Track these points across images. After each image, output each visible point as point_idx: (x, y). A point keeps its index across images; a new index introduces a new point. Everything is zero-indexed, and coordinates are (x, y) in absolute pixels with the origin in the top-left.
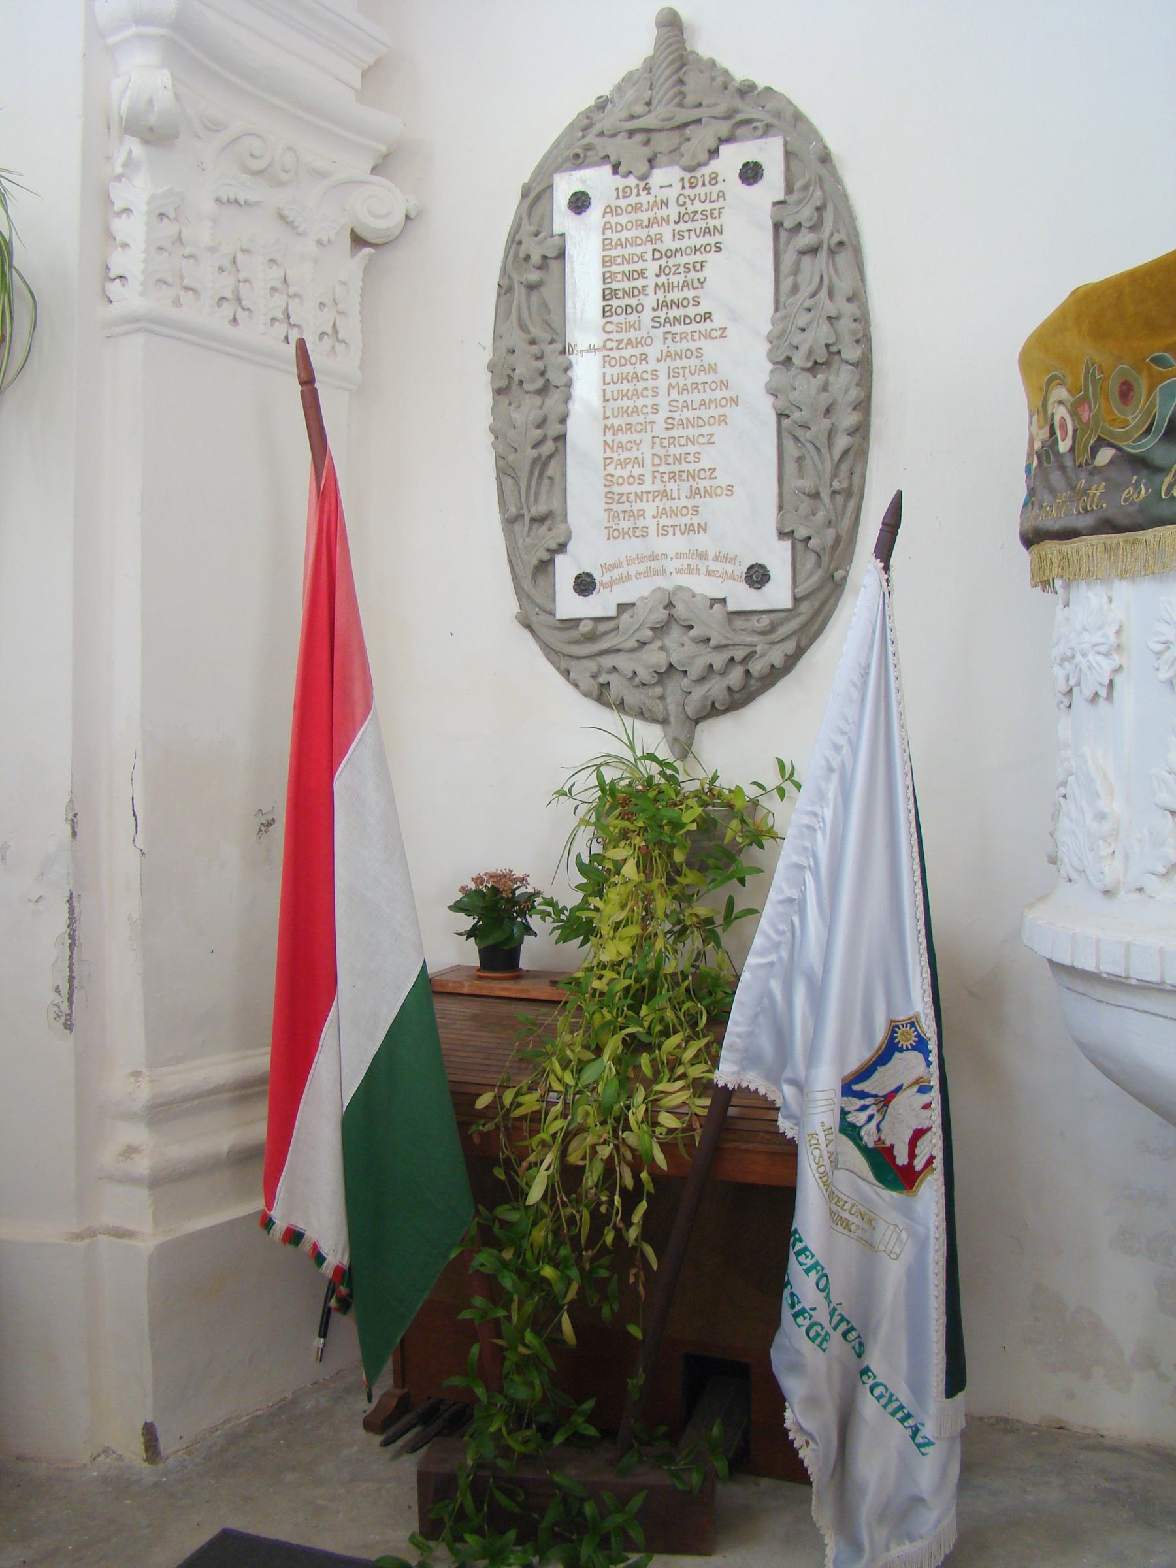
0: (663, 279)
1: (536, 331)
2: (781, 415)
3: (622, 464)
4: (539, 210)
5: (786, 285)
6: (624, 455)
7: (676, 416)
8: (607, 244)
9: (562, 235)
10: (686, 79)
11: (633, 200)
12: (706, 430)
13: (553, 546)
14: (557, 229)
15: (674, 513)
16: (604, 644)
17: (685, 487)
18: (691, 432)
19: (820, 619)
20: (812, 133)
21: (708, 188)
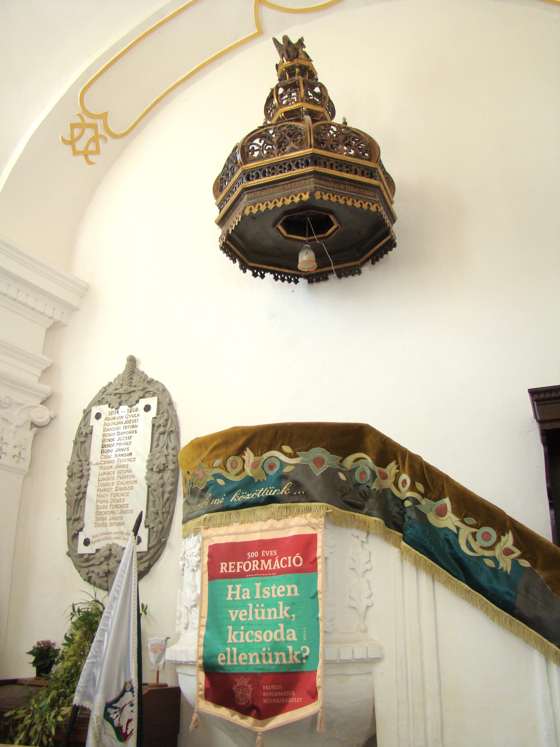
0: (119, 442)
1: (82, 458)
2: (149, 487)
3: (101, 502)
4: (87, 418)
5: (155, 444)
6: (103, 499)
7: (119, 486)
8: (105, 430)
9: (92, 426)
10: (133, 378)
11: (113, 416)
12: (127, 491)
13: (78, 529)
14: (91, 425)
15: (115, 519)
16: (91, 563)
17: (119, 510)
18: (123, 492)
19: (157, 555)
20: (169, 395)
21: (135, 412)
